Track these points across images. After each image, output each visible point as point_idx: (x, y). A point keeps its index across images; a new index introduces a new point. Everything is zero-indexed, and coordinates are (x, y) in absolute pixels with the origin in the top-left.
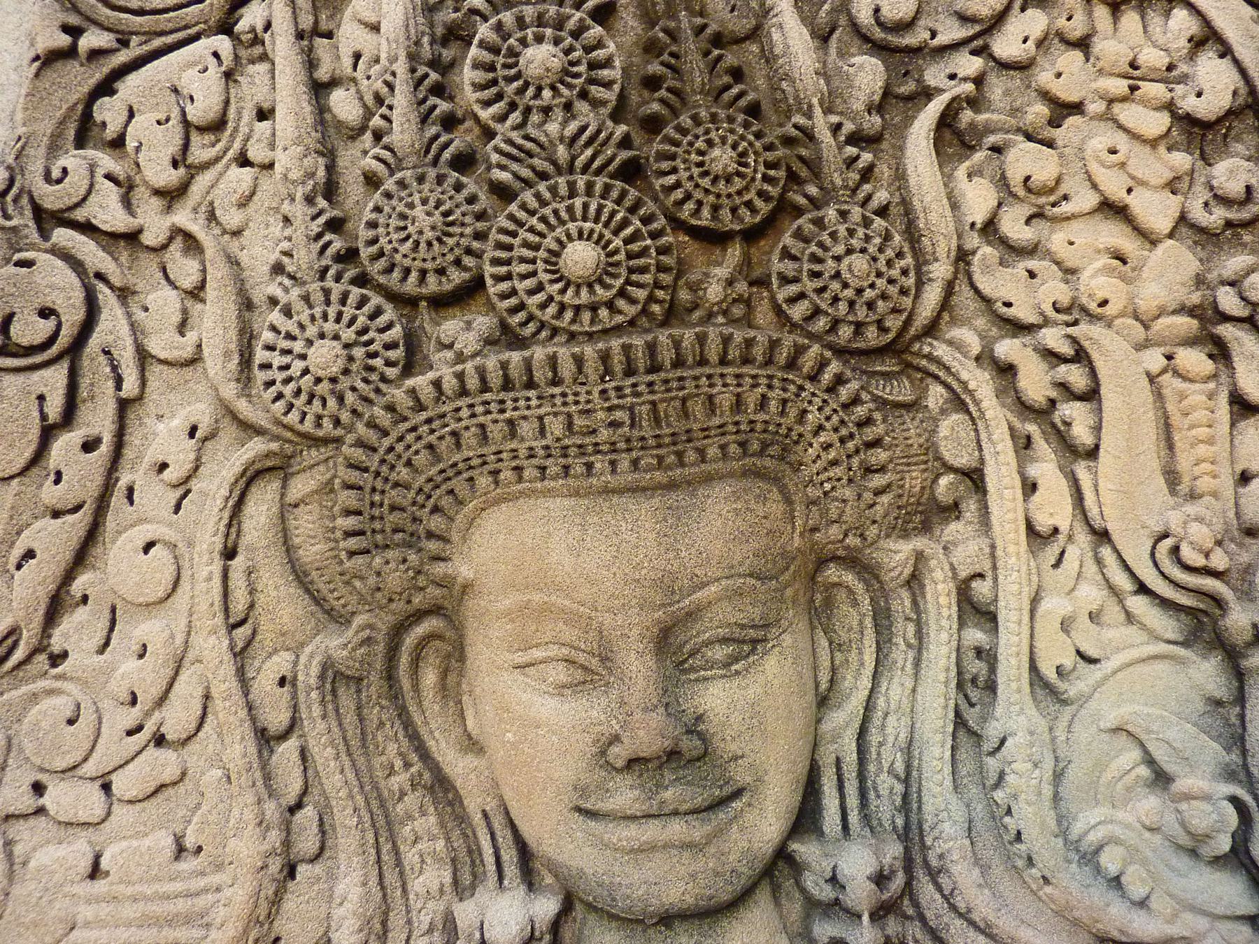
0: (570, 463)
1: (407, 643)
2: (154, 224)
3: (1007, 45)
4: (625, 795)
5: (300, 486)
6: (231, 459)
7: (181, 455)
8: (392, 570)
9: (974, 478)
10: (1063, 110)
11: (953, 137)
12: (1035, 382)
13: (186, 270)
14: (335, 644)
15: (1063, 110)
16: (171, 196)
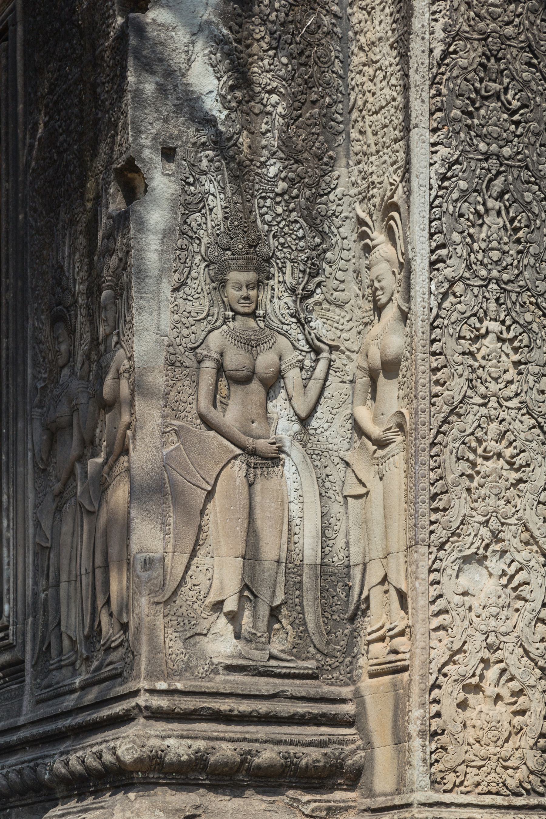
0: (239, 268)
1: (221, 284)
2: (194, 236)
3: (281, 226)
4: (243, 301)
5: (211, 268)
6: (203, 265)
7: (198, 263)
8: (220, 277)
9: (273, 275)
10: (285, 234)
11: (274, 237)
12: (280, 265)
13: (198, 242)
14: (214, 285)
15: (285, 234)
16: (195, 233)
